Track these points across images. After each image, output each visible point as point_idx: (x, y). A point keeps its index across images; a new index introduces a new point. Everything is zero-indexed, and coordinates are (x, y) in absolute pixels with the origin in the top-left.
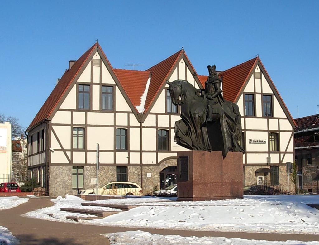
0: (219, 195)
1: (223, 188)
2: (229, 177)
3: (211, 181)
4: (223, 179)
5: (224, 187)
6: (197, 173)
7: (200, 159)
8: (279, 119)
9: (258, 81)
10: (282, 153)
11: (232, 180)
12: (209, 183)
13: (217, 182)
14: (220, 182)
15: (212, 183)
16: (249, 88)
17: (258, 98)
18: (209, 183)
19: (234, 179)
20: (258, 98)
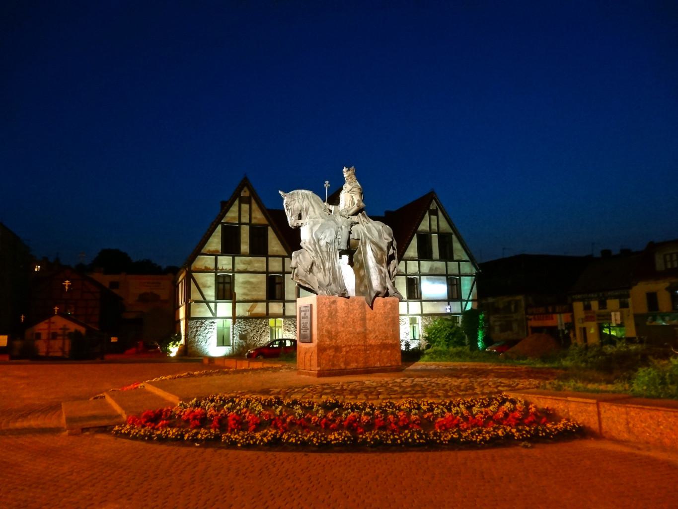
0: (361, 365)
1: (368, 354)
2: (376, 336)
3: (348, 344)
4: (368, 340)
5: (368, 352)
6: (324, 331)
7: (329, 309)
8: (459, 261)
9: (434, 217)
10: (465, 301)
11: (381, 341)
12: (344, 347)
13: (358, 345)
14: (363, 345)
15: (350, 346)
16: (424, 226)
17: (435, 239)
18: (344, 347)
19: (385, 340)
20: (435, 239)
